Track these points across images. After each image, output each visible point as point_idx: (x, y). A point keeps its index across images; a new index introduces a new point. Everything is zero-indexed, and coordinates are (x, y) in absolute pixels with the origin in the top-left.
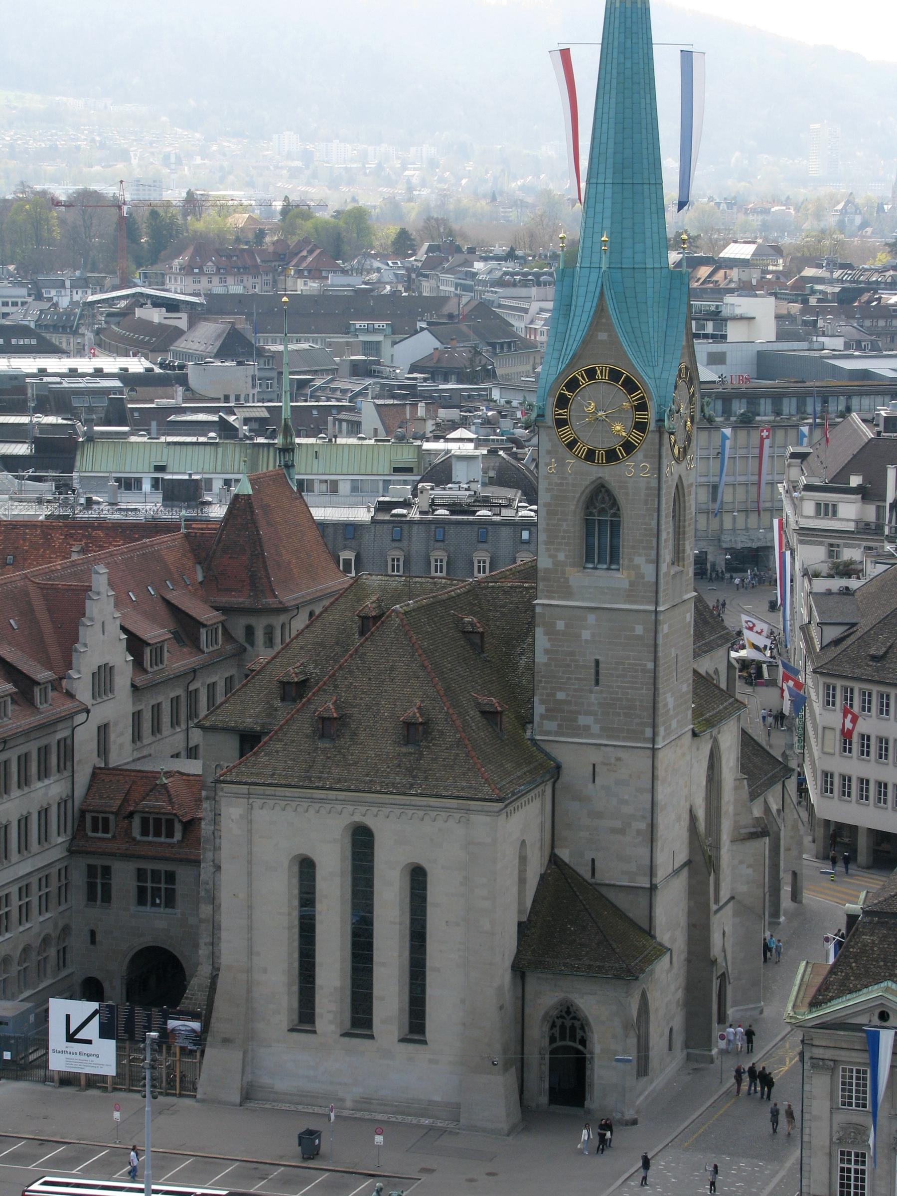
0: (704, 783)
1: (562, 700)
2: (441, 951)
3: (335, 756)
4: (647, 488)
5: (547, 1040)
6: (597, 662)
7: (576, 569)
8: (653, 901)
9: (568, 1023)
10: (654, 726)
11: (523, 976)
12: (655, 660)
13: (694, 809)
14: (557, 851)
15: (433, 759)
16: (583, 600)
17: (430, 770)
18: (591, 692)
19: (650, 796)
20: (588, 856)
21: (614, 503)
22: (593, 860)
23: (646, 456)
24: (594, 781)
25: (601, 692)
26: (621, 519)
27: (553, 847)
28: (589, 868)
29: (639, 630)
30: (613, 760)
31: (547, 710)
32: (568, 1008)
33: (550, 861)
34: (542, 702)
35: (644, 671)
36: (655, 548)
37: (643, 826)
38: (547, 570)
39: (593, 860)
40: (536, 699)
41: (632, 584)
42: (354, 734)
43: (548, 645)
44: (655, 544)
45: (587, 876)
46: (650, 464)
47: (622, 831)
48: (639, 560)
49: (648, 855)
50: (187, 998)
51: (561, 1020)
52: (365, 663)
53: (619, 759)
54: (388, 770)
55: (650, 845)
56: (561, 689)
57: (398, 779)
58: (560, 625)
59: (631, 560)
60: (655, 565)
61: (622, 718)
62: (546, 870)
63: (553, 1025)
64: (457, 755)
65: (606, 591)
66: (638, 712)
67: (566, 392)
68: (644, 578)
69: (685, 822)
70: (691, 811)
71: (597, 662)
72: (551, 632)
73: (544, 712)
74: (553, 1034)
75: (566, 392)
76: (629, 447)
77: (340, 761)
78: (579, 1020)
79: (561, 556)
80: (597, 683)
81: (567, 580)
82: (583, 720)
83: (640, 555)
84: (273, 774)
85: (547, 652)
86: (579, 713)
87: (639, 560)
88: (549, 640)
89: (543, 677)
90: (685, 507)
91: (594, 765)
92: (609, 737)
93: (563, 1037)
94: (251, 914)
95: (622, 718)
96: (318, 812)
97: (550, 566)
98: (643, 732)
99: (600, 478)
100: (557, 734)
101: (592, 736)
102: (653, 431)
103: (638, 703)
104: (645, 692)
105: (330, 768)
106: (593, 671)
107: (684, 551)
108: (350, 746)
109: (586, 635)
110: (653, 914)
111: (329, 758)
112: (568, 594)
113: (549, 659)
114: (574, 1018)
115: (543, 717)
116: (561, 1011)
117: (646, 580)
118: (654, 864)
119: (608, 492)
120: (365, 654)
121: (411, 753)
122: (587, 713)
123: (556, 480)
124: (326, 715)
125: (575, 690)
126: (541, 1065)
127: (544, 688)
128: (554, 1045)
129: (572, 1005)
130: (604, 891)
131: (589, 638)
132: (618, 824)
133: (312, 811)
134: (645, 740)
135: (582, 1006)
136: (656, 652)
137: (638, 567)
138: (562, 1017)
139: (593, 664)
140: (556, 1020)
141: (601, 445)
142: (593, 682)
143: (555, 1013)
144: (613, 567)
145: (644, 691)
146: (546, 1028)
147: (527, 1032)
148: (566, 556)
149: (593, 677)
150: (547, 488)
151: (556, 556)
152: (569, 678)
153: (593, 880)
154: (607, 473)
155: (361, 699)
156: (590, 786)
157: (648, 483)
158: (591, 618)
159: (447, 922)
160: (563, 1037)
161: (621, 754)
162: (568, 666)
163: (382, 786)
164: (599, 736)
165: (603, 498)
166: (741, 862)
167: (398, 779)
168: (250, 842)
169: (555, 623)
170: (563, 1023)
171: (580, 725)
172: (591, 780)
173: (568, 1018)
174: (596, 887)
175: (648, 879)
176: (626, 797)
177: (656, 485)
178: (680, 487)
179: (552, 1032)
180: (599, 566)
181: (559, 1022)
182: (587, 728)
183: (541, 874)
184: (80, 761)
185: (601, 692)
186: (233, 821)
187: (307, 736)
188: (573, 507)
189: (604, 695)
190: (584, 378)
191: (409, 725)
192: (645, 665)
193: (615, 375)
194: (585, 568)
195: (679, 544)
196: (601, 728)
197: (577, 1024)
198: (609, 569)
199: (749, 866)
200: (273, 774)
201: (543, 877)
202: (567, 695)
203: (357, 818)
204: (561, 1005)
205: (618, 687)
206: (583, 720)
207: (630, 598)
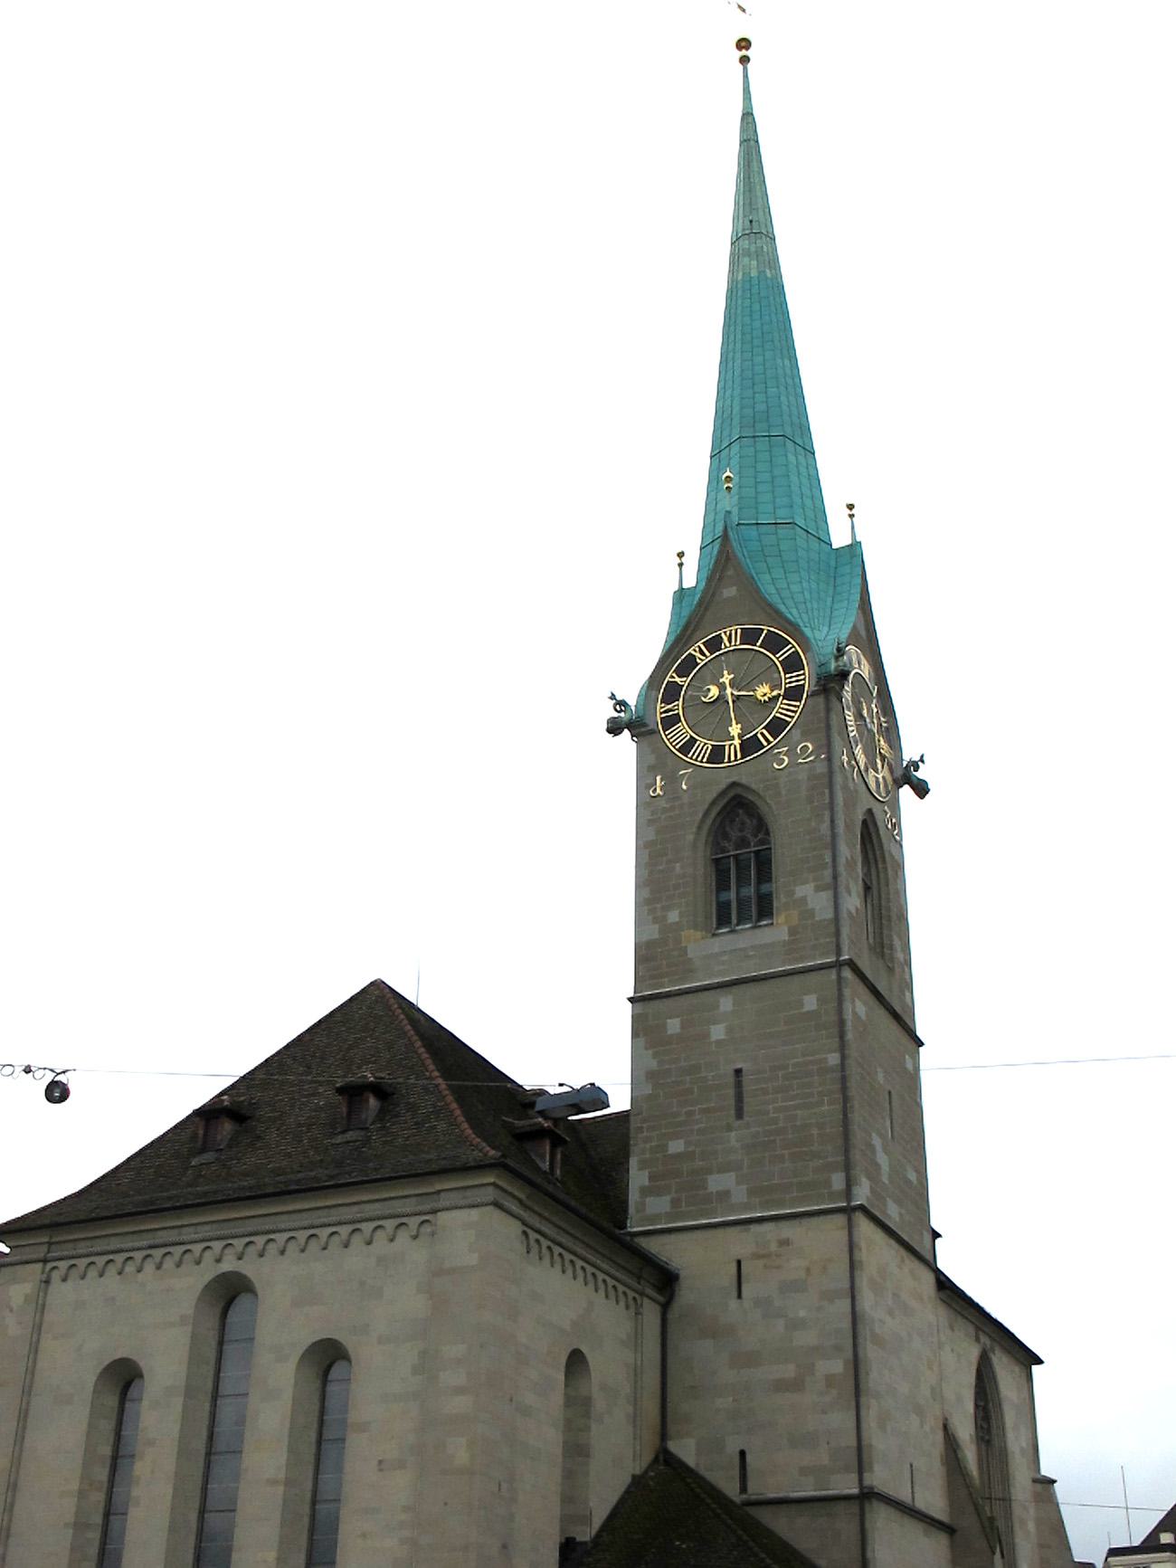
1: (678, 1156)
2: (364, 1536)
7: (699, 934)
8: (868, 1525)
10: (848, 1167)
12: (843, 1048)
13: (951, 1426)
14: (672, 1446)
18: (729, 1128)
19: (848, 1301)
20: (733, 1446)
21: (762, 827)
22: (742, 1454)
24: (739, 1296)
27: (664, 1436)
29: (810, 1003)
30: (773, 1247)
31: (651, 1178)
34: (643, 1165)
36: (830, 864)
37: (837, 1366)
39: (742, 1454)
40: (633, 1162)
41: (793, 931)
43: (653, 1064)
44: (828, 859)
45: (730, 1489)
46: (812, 745)
47: (796, 1385)
49: (852, 1424)
53: (785, 1243)
55: (853, 1403)
56: (676, 1136)
58: (674, 1026)
62: (646, 1472)
64: (434, 1127)
65: (751, 953)
67: (678, 680)
70: (945, 1427)
71: (738, 1072)
73: (647, 1183)
75: (678, 680)
79: (673, 916)
80: (739, 1114)
86: (709, 1171)
88: (655, 1055)
91: (739, 1263)
92: (765, 1205)
94: (12, 1505)
96: (159, 1267)
97: (656, 936)
98: (828, 1183)
99: (734, 784)
100: (672, 1216)
101: (732, 1209)
103: (815, 1132)
104: (830, 1109)
106: (731, 1092)
107: (891, 947)
109: (718, 1032)
110: (869, 1554)
112: (689, 972)
118: (865, 1443)
122: (723, 1169)
123: (663, 804)
127: (647, 1140)
132: (789, 1371)
133: (149, 1267)
134: (833, 1196)
136: (842, 1035)
137: (804, 900)
139: (731, 1080)
145: (825, 1108)
148: (681, 915)
149: (732, 1102)
150: (649, 820)
151: (665, 918)
152: (690, 1114)
156: (733, 1303)
158: (726, 1002)
159: (380, 1462)
161: (787, 1230)
164: (747, 1207)
165: (743, 823)
168: (35, 1349)
169: (665, 1025)
171: (712, 1193)
172: (735, 1293)
174: (752, 1511)
175: (854, 1476)
176: (802, 1313)
182: (724, 1195)
183: (634, 1477)
185: (748, 1126)
186: (11, 1311)
188: (691, 837)
189: (753, 1130)
194: (714, 935)
195: (881, 933)
196: (751, 1192)
198: (755, 927)
202: (687, 1143)
203: (228, 1265)
206: (716, 1183)
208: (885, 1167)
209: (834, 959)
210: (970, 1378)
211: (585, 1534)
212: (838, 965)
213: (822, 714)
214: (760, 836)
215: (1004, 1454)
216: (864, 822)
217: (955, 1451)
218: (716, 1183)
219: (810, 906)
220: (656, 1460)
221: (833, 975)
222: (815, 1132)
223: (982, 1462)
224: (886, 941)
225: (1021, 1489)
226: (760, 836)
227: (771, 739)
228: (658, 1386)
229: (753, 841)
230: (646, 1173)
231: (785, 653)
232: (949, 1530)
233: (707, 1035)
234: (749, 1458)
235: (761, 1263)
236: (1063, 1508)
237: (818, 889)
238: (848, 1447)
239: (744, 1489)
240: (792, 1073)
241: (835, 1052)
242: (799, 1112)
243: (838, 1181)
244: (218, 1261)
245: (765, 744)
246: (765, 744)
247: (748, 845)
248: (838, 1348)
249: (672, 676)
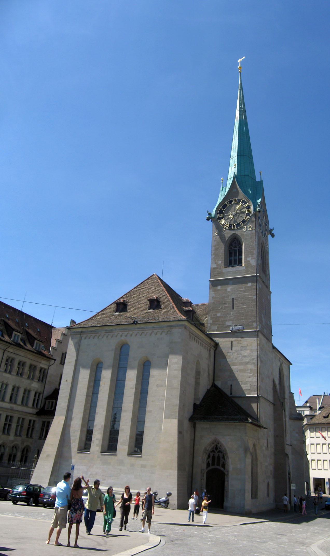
0: (278, 377)
5: (205, 465)
9: (216, 455)
19: (256, 353)
22: (231, 385)
28: (229, 390)
32: (217, 446)
39: (231, 385)
44: (255, 252)
45: (228, 393)
51: (213, 453)
60: (255, 260)
63: (209, 456)
68: (251, 265)
69: (271, 384)
74: (209, 462)
78: (222, 452)
83: (249, 257)
87: (248, 259)
93: (213, 464)
98: (253, 325)
114: (219, 452)
116: (213, 448)
117: (252, 265)
126: (201, 479)
128: (209, 468)
129: (218, 443)
130: (236, 400)
132: (242, 367)
135: (223, 442)
138: (213, 451)
140: (210, 453)
143: (210, 449)
146: (205, 457)
153: (231, 395)
170: (214, 455)
173: (216, 452)
174: (233, 398)
179: (208, 460)
181: (211, 455)
189: (236, 312)
197: (221, 455)
199: (297, 433)
204: (213, 443)
207: (246, 272)
208: (264, 322)
209: (255, 275)
210: (278, 370)
212: (256, 276)
214: (239, 246)
215: (284, 387)
216: (262, 243)
217: (275, 387)
219: (250, 262)
220: (212, 386)
223: (280, 389)
224: (265, 270)
225: (287, 396)
226: (239, 246)
227: (243, 224)
228: (213, 369)
229: (238, 246)
232: (274, 404)
234: (233, 386)
235: (237, 342)
236: (295, 401)
237: (252, 259)
238: (255, 386)
239: (231, 394)
240: (245, 300)
241: (255, 295)
243: (255, 325)
245: (241, 225)
246: (241, 225)
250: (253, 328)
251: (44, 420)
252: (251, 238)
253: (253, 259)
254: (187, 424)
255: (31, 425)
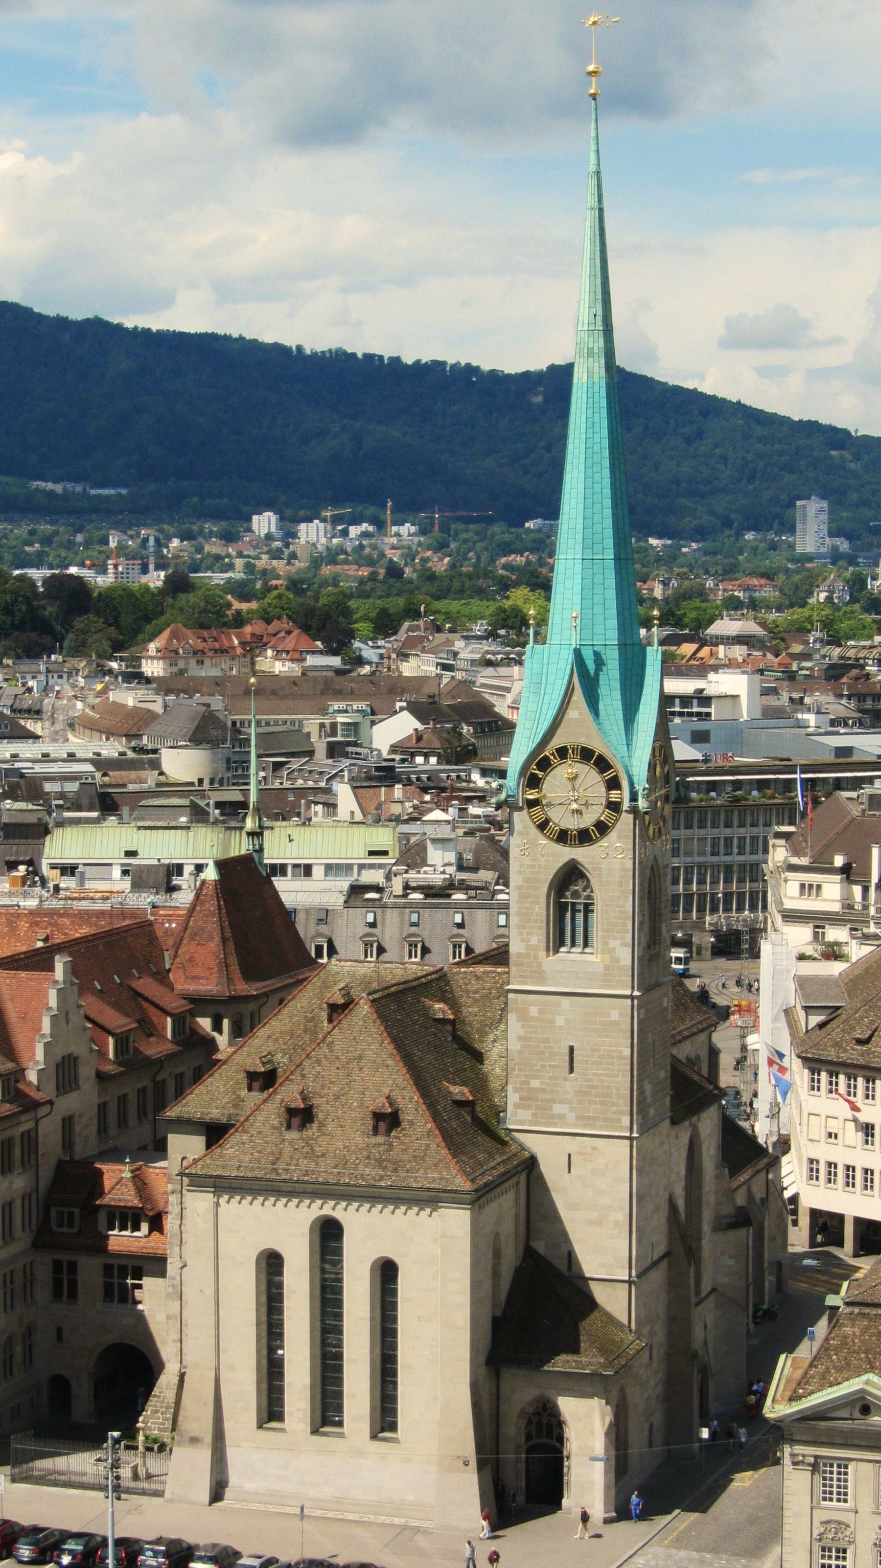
0: (683, 1172)
3: (303, 1147)
4: (623, 870)
5: (523, 1437)
6: (572, 1049)
11: (497, 1374)
15: (403, 1150)
16: (556, 985)
17: (400, 1161)
18: (566, 1079)
21: (588, 886)
23: (619, 837)
24: (569, 1172)
25: (576, 1080)
26: (595, 901)
28: (566, 1261)
29: (615, 1016)
30: (589, 1150)
31: (521, 1099)
32: (545, 1404)
33: (525, 1254)
34: (516, 1090)
35: (622, 1058)
38: (519, 955)
40: (510, 1088)
41: (606, 968)
42: (322, 1125)
48: (614, 943)
50: (155, 1396)
52: (332, 1051)
53: (594, 1148)
54: (357, 1161)
56: (536, 1077)
57: (367, 1171)
58: (534, 1011)
59: (605, 944)
61: (598, 1106)
62: (521, 1263)
63: (529, 1423)
64: (428, 1146)
66: (615, 1100)
67: (537, 772)
68: (618, 961)
71: (572, 1049)
72: (524, 1018)
73: (517, 1100)
75: (537, 772)
76: (602, 828)
77: (307, 1153)
80: (571, 1070)
81: (540, 965)
82: (558, 1109)
84: (240, 1167)
85: (520, 1038)
86: (554, 1101)
88: (523, 1026)
89: (516, 1064)
90: (660, 888)
91: (570, 1155)
92: (585, 1126)
93: (539, 1434)
95: (598, 1106)
97: (523, 951)
98: (619, 1121)
100: (531, 1123)
102: (626, 811)
105: (298, 1160)
106: (567, 1058)
107: (660, 934)
108: (318, 1137)
109: (560, 1021)
111: (296, 1149)
112: (542, 980)
113: (522, 1046)
115: (517, 1106)
117: (622, 963)
119: (582, 875)
120: (332, 1042)
121: (380, 1144)
122: (561, 1102)
124: (293, 1106)
125: (550, 1078)
127: (519, 1076)
128: (531, 1443)
129: (548, 1401)
131: (563, 1024)
137: (611, 951)
139: (567, 1051)
141: (572, 824)
142: (567, 1069)
143: (531, 1410)
144: (587, 950)
145: (620, 1078)
146: (523, 1423)
147: (502, 1430)
149: (567, 1064)
150: (519, 871)
151: (528, 941)
152: (543, 1066)
154: (580, 854)
155: (329, 1089)
156: (566, 1175)
157: (623, 864)
158: (566, 1001)
160: (539, 1434)
162: (543, 1053)
163: (351, 1179)
164: (574, 1126)
166: (723, 1253)
167: (367, 1171)
177: (631, 867)
178: (655, 868)
180: (573, 950)
182: (562, 1117)
184: (43, 1155)
185: (576, 1080)
186: (198, 1214)
187: (274, 1128)
190: (555, 758)
191: (378, 1116)
192: (621, 1051)
193: (586, 754)
196: (578, 1117)
197: (554, 1421)
198: (582, 953)
200: (240, 1167)
201: (518, 1272)
202: (542, 1083)
204: (538, 1401)
205: (594, 1074)
209: (628, 992)
211: (499, 1313)
213: (632, 827)
218: (558, 1109)
221: (629, 1001)
222: (614, 1091)
230: (517, 1095)
231: (609, 775)
233: (553, 1021)
242: (606, 1079)
243: (626, 1120)
244: (321, 1208)
247: (579, 897)
248: (621, 1208)
249: (533, 768)
250: (622, 1129)
251: (57, 1256)
252: (620, 884)
253: (626, 945)
254: (483, 1371)
255: (28, 1274)
